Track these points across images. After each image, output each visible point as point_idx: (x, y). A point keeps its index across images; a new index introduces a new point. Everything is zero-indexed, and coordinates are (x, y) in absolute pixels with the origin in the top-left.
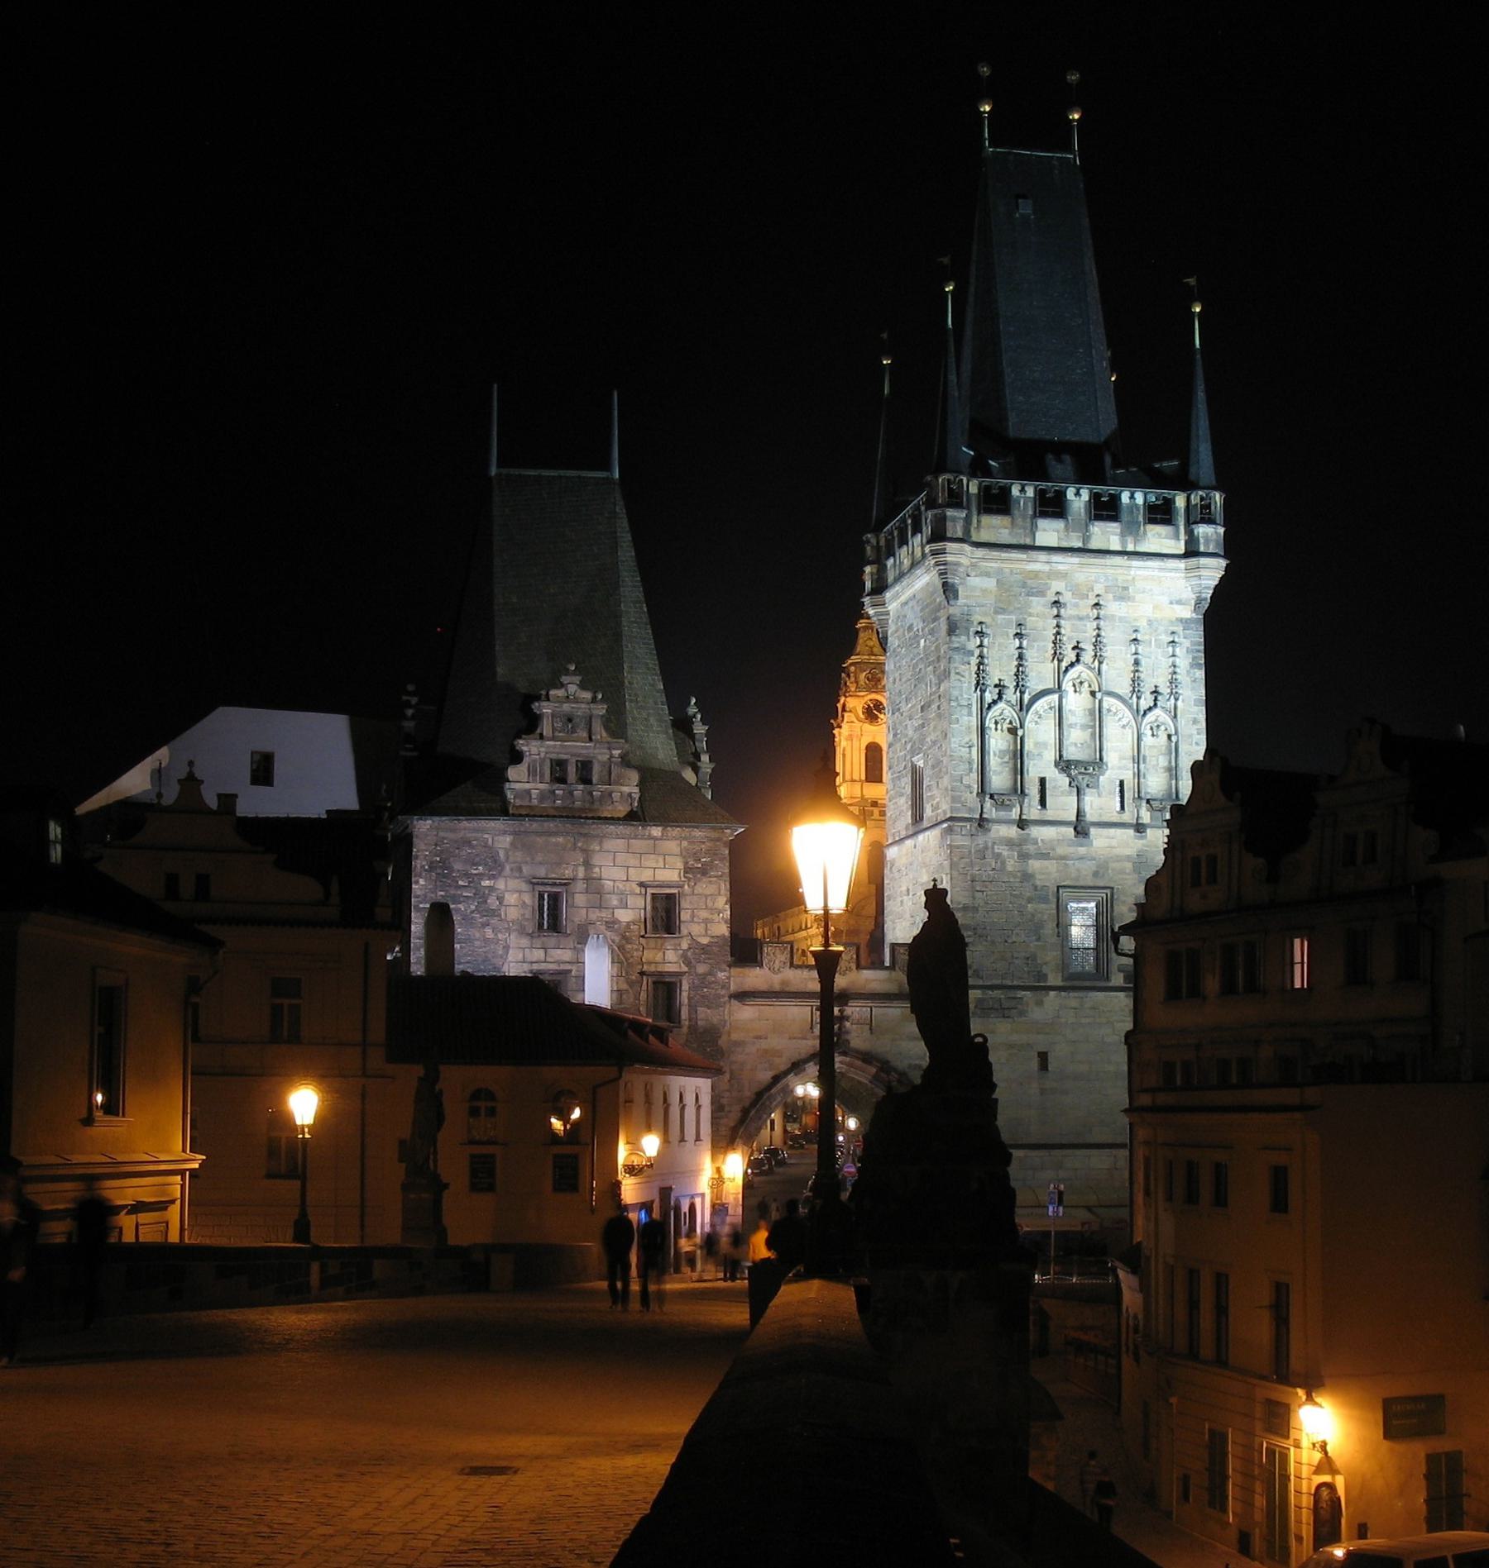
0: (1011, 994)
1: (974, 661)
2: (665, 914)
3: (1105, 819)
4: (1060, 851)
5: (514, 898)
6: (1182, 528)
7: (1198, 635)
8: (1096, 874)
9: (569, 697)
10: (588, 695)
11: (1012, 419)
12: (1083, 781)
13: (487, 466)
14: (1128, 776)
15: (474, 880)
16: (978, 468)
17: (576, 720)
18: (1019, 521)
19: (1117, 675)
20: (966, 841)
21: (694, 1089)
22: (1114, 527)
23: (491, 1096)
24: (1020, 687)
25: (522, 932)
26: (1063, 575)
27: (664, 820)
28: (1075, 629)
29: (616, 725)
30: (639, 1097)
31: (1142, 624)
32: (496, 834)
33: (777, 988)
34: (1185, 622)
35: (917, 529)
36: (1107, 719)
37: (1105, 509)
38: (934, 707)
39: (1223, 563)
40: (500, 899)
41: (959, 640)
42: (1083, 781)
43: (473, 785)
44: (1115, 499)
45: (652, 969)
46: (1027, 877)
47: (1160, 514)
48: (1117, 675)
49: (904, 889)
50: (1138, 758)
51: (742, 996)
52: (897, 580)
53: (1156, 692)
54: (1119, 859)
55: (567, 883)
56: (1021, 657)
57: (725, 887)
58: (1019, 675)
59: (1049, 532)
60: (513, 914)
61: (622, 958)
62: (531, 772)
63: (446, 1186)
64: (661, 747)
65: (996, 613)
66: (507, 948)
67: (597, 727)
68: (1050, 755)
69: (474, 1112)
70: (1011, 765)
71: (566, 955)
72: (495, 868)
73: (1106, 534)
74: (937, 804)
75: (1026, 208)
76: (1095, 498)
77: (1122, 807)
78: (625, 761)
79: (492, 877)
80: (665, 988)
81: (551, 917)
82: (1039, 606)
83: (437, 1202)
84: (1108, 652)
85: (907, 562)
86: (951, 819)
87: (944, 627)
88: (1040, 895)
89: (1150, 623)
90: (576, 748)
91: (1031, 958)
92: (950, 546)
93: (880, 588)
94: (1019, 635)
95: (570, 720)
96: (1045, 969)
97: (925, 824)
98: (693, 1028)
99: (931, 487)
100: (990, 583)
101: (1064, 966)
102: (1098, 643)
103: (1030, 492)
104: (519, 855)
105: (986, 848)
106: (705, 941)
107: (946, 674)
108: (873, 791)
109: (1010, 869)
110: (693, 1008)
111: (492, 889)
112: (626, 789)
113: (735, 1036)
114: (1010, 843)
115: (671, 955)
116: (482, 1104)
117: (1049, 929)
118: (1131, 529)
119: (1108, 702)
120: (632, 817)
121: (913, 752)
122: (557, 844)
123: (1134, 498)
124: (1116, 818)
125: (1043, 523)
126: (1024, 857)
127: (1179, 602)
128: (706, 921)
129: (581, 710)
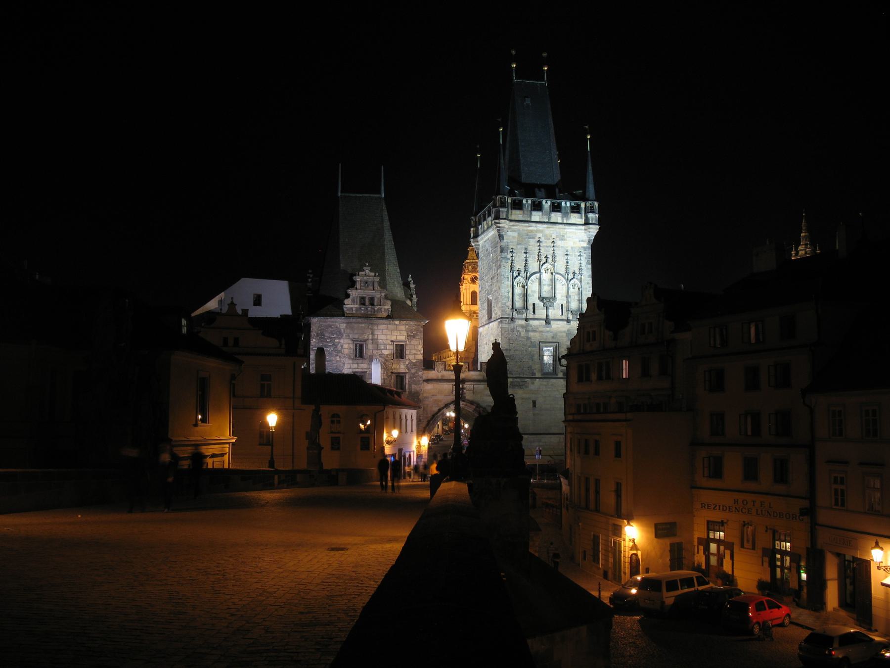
1: (510, 262)
2: (400, 352)
4: (540, 329)
5: (346, 346)
7: (589, 253)
9: (366, 275)
10: (373, 274)
11: (523, 176)
13: (337, 193)
15: (332, 339)
16: (511, 193)
19: (560, 267)
20: (507, 326)
21: (411, 414)
22: (559, 214)
23: (338, 416)
24: (526, 271)
25: (350, 358)
26: (541, 231)
27: (400, 318)
29: (383, 284)
30: (391, 417)
31: (569, 249)
32: (340, 323)
34: (584, 248)
35: (489, 215)
37: (556, 208)
39: (598, 227)
40: (342, 346)
41: (504, 255)
42: (548, 304)
43: (331, 305)
44: (560, 204)
46: (528, 338)
47: (576, 210)
48: (560, 267)
50: (568, 296)
51: (428, 381)
52: (482, 233)
53: (574, 273)
54: (561, 332)
55: (365, 341)
57: (421, 342)
58: (526, 267)
59: (536, 216)
60: (346, 351)
61: (385, 367)
62: (353, 301)
64: (399, 292)
67: (376, 285)
68: (537, 295)
69: (333, 422)
71: (365, 366)
72: (340, 335)
73: (557, 217)
74: (497, 312)
75: (528, 101)
76: (553, 204)
78: (386, 297)
80: (400, 378)
81: (360, 353)
82: (533, 242)
83: (320, 454)
84: (557, 259)
85: (486, 227)
87: (499, 249)
88: (533, 345)
90: (369, 292)
91: (530, 367)
92: (501, 221)
93: (476, 236)
94: (525, 253)
98: (410, 392)
99: (495, 200)
100: (516, 234)
101: (542, 370)
102: (553, 255)
103: (530, 202)
104: (348, 331)
106: (414, 361)
107: (500, 266)
108: (474, 308)
110: (410, 385)
114: (522, 326)
116: (335, 419)
117: (536, 357)
118: (565, 215)
119: (557, 276)
120: (388, 317)
121: (488, 294)
123: (566, 204)
125: (534, 213)
126: (527, 331)
129: (370, 279)
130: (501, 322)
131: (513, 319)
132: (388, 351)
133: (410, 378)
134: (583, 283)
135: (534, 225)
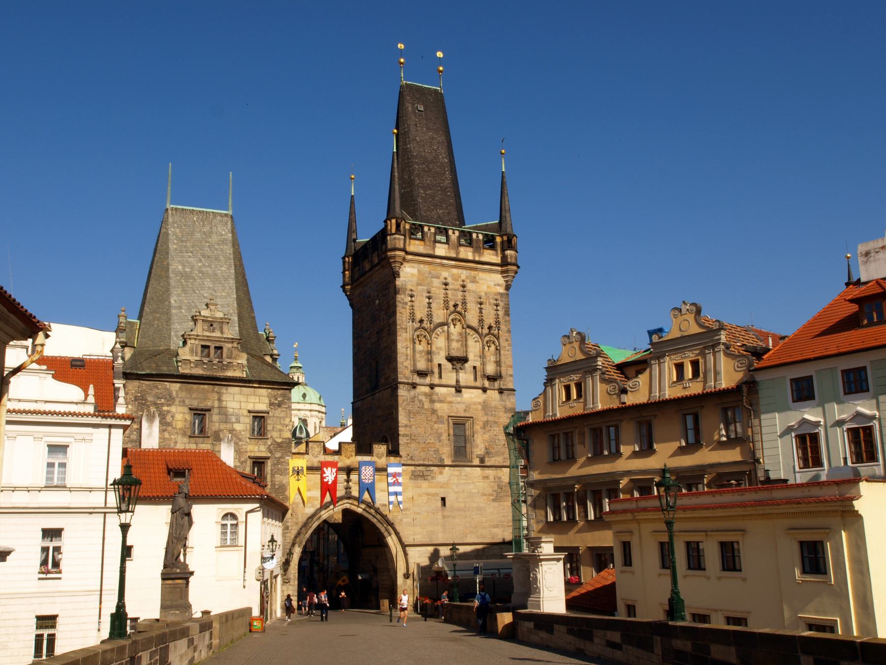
0: (428, 468)
1: (408, 307)
3: (469, 384)
4: (449, 399)
6: (499, 251)
8: (465, 410)
12: (459, 365)
17: (215, 325)
18: (428, 243)
25: (184, 434)
31: (483, 294)
34: (501, 294)
36: (469, 337)
45: (253, 455)
46: (434, 411)
48: (472, 318)
50: (483, 356)
53: (490, 328)
54: (475, 404)
55: (209, 410)
56: (429, 307)
58: (430, 316)
60: (180, 425)
63: (192, 573)
66: (176, 443)
68: (443, 354)
70: (426, 357)
72: (171, 400)
77: (476, 379)
79: (169, 405)
84: (469, 306)
88: (439, 420)
89: (486, 294)
95: (212, 325)
96: (444, 457)
100: (414, 271)
103: (433, 230)
105: (415, 397)
106: (279, 440)
107: (394, 313)
109: (426, 407)
111: (169, 412)
112: (240, 362)
114: (426, 394)
115: (263, 448)
122: (204, 389)
124: (473, 384)
125: (438, 245)
126: (432, 401)
127: (498, 285)
128: (280, 430)
131: (414, 386)
132: (244, 426)
133: (273, 465)
134: (501, 340)
135: (438, 261)
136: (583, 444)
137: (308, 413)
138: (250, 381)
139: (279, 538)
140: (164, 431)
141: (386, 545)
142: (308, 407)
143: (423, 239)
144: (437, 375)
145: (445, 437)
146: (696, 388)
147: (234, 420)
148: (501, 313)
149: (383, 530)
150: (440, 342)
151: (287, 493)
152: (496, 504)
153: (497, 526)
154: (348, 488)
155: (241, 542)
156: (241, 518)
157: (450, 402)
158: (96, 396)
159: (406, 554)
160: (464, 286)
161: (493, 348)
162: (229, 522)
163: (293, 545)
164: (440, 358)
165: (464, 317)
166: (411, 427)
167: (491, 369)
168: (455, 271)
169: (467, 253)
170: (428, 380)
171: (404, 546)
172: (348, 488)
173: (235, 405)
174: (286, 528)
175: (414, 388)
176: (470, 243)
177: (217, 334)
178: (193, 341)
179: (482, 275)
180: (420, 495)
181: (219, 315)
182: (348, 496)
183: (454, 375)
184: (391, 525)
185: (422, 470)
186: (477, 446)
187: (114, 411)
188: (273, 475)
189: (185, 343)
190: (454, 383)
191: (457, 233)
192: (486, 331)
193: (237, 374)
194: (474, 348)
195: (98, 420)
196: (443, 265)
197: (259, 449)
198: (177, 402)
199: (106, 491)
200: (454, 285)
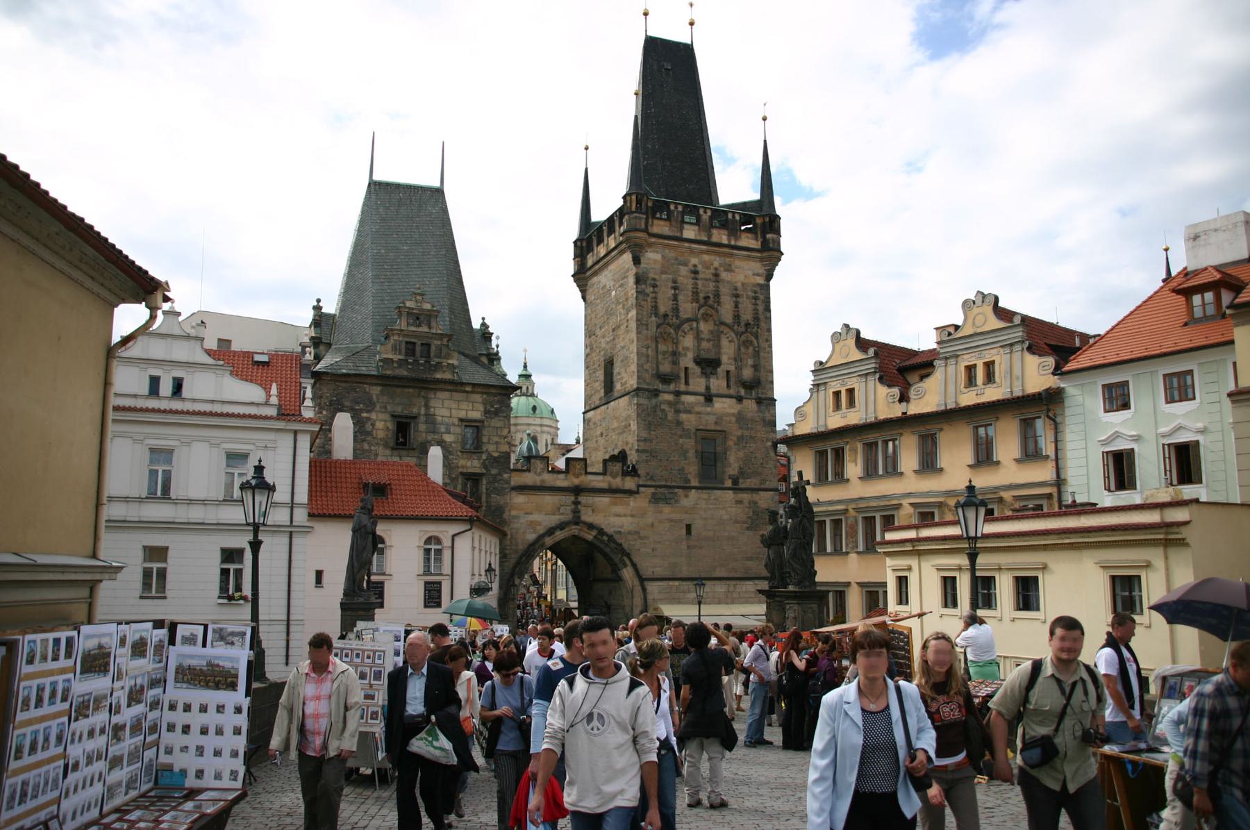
4: (697, 409)
8: (716, 423)
12: (709, 370)
14: (732, 368)
19: (726, 312)
25: (386, 446)
28: (703, 285)
31: (739, 285)
33: (538, 484)
38: (623, 327)
40: (373, 425)
46: (679, 423)
48: (726, 312)
49: (598, 433)
50: (737, 359)
54: (728, 415)
55: (415, 418)
56: (675, 298)
60: (381, 434)
65: (663, 273)
66: (376, 455)
67: (433, 324)
68: (690, 355)
72: (370, 406)
77: (728, 386)
79: (368, 412)
86: (638, 389)
87: (631, 280)
88: (686, 434)
91: (682, 469)
97: (616, 394)
100: (658, 257)
103: (680, 208)
106: (496, 455)
111: (368, 419)
113: (514, 513)
114: (669, 403)
115: (476, 463)
124: (724, 391)
125: (686, 226)
126: (677, 412)
127: (758, 275)
128: (497, 443)
130: (637, 395)
131: (656, 393)
135: (687, 245)
136: (855, 461)
137: (538, 429)
138: (462, 384)
139: (496, 566)
140: (363, 441)
141: (619, 579)
142: (538, 421)
143: (668, 219)
144: (683, 381)
145: (691, 454)
146: (992, 394)
147: (443, 430)
148: (761, 308)
149: (617, 560)
150: (688, 341)
151: (505, 516)
152: (750, 533)
153: (750, 559)
154: (576, 512)
155: (446, 569)
156: (447, 542)
157: (698, 413)
158: (279, 396)
159: (644, 590)
160: (716, 275)
161: (751, 349)
162: (433, 547)
163: (512, 575)
164: (687, 361)
165: (717, 311)
166: (651, 441)
167: (747, 373)
168: (706, 257)
169: (721, 236)
170: (672, 387)
171: (642, 580)
172: (576, 512)
173: (446, 412)
174: (503, 556)
175: (657, 395)
176: (724, 225)
177: (424, 329)
178: (396, 337)
179: (737, 263)
180: (660, 522)
181: (427, 306)
182: (577, 521)
183: (703, 381)
184: (628, 555)
185: (664, 494)
186: (730, 465)
187: (300, 415)
188: (488, 495)
189: (387, 338)
190: (702, 389)
191: (709, 213)
192: (742, 329)
193: (448, 376)
194: (728, 350)
195: (281, 425)
196: (692, 251)
197: (472, 465)
198: (378, 408)
199: (292, 508)
200: (705, 274)
